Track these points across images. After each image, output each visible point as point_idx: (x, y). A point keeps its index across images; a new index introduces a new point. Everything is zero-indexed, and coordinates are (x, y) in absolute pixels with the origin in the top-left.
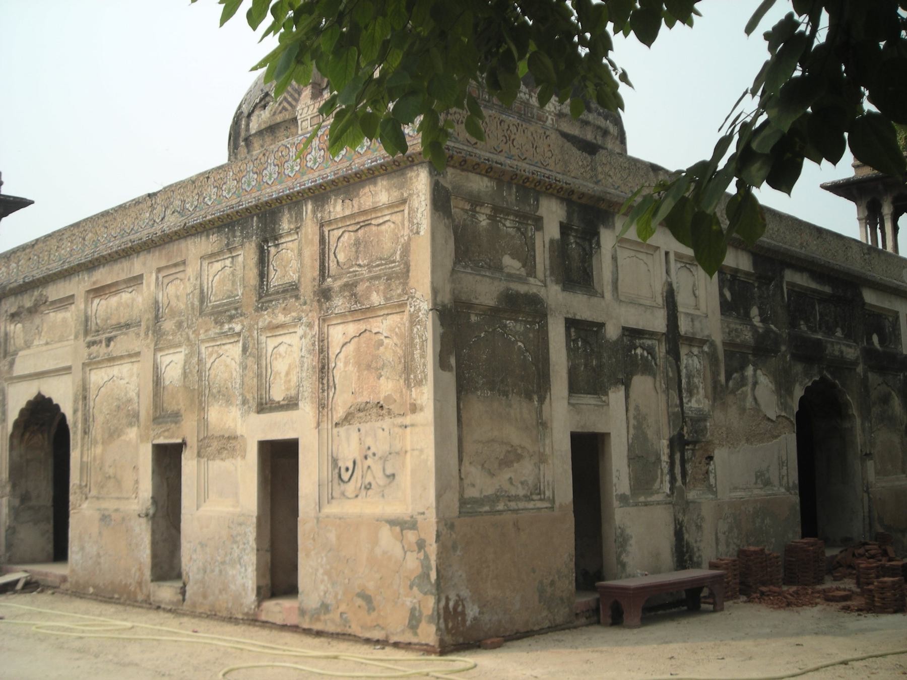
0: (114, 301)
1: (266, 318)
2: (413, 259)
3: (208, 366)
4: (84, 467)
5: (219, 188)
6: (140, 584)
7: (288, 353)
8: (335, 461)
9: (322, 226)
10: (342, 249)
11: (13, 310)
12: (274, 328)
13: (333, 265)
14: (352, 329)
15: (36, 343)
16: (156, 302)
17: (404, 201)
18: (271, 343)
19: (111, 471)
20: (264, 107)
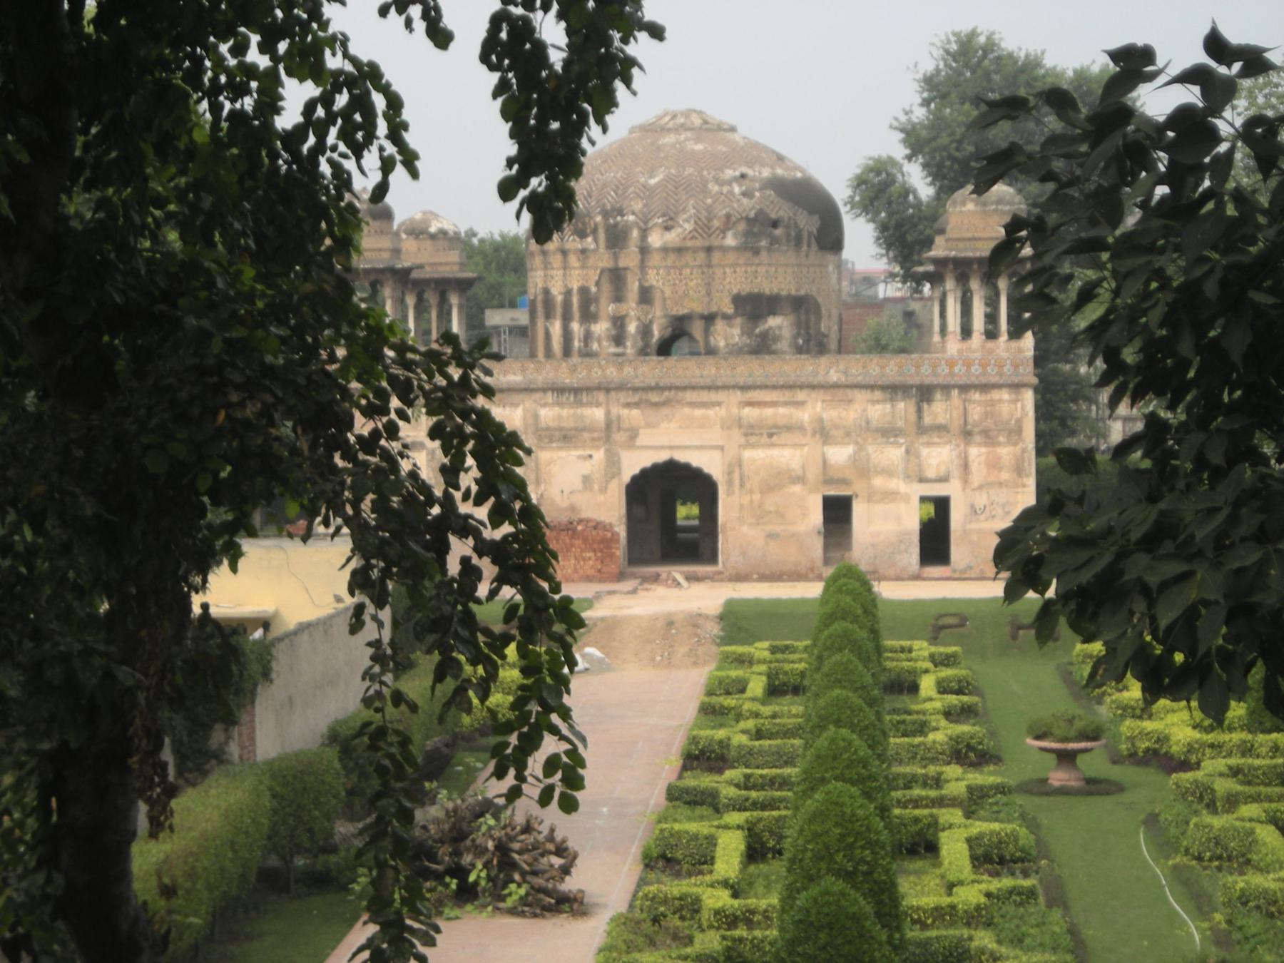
0: (769, 412)
1: (925, 438)
2: (1024, 425)
3: (873, 456)
4: (741, 506)
5: (882, 368)
6: (812, 569)
7: (938, 456)
8: (972, 506)
9: (965, 401)
10: (975, 413)
11: (630, 400)
12: (928, 444)
13: (970, 420)
14: (984, 450)
15: (664, 425)
16: (821, 420)
17: (1018, 400)
18: (925, 451)
19: (772, 509)
20: (668, 228)
